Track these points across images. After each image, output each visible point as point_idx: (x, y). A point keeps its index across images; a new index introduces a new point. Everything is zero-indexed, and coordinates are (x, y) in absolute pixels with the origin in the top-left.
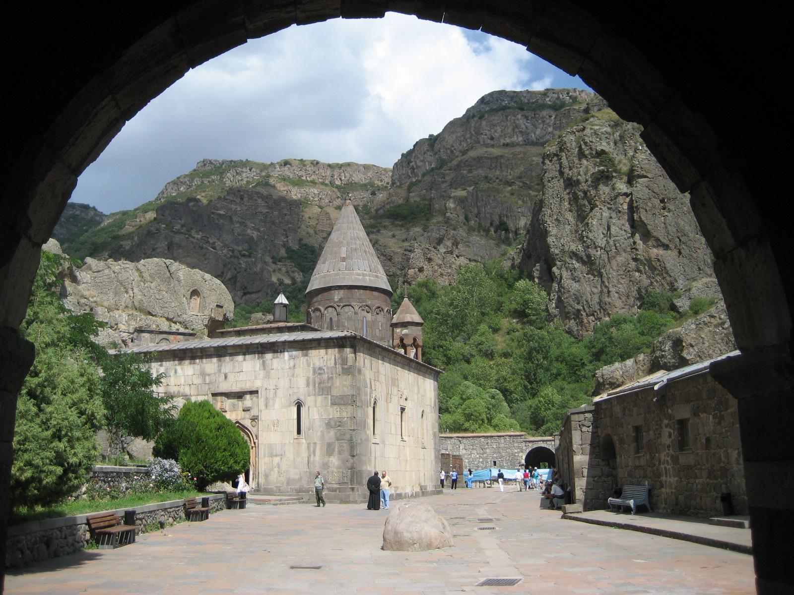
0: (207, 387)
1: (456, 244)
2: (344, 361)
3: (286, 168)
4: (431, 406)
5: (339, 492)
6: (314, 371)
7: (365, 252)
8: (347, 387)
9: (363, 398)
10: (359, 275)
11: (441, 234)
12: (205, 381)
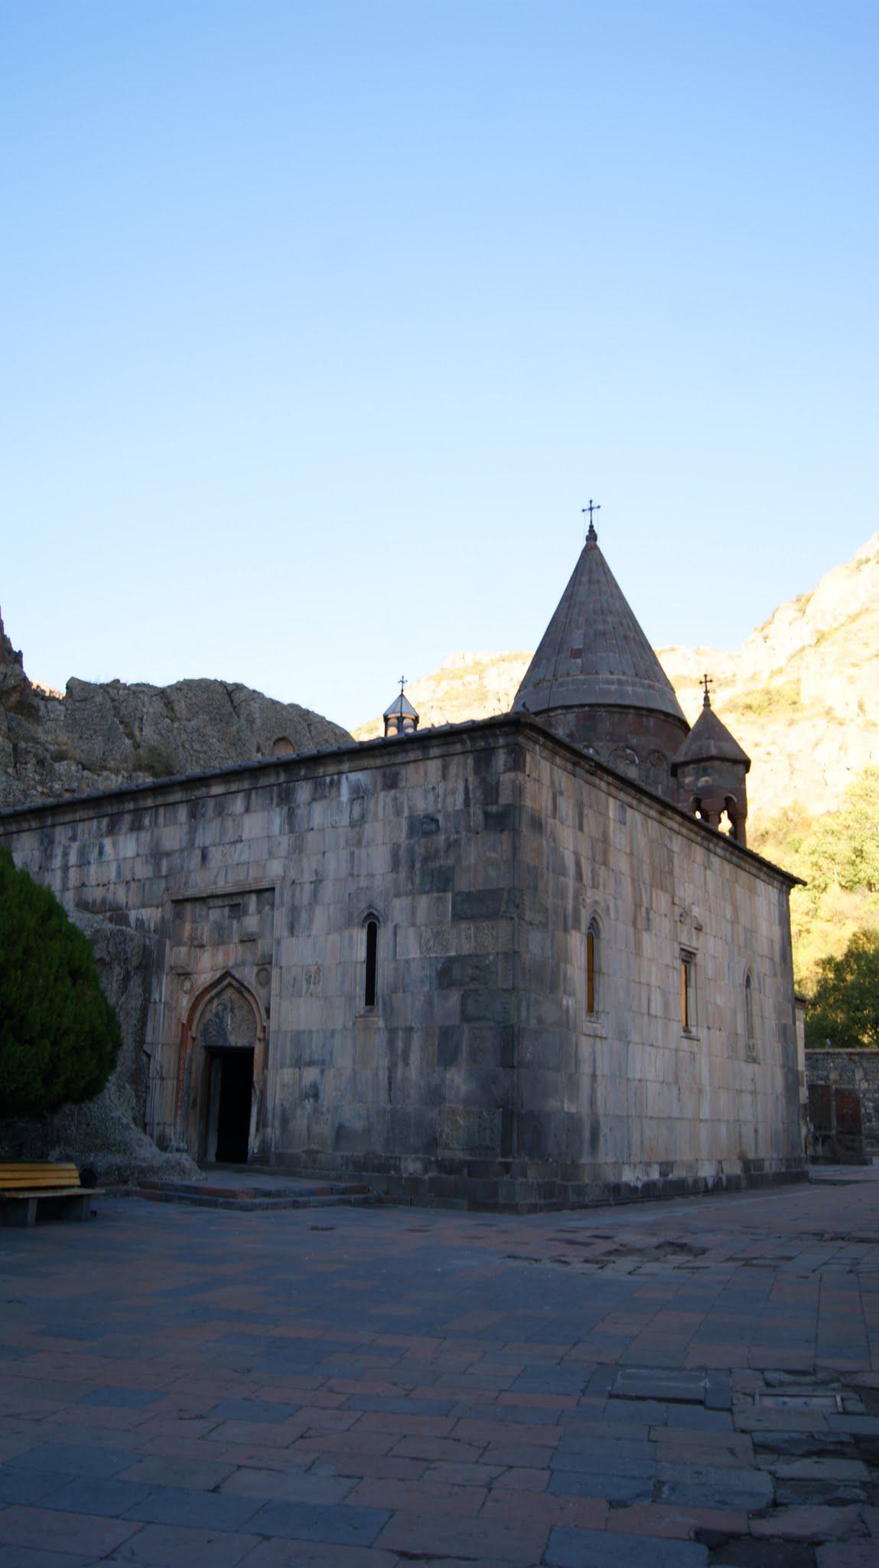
2: (490, 791)
4: (772, 959)
5: (469, 1174)
6: (412, 830)
7: (626, 637)
9: (550, 902)
12: (159, 871)
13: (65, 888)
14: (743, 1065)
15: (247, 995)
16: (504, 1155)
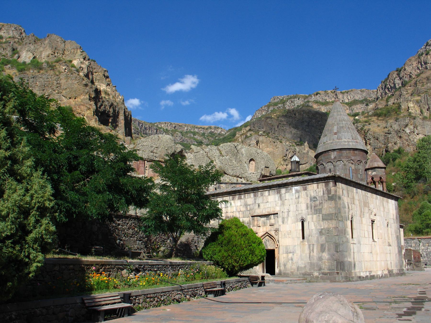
0: (248, 212)
1: (415, 127)
2: (329, 192)
3: (318, 96)
6: (311, 200)
7: (349, 128)
9: (343, 215)
10: (345, 142)
11: (407, 122)
14: (387, 247)
16: (337, 270)
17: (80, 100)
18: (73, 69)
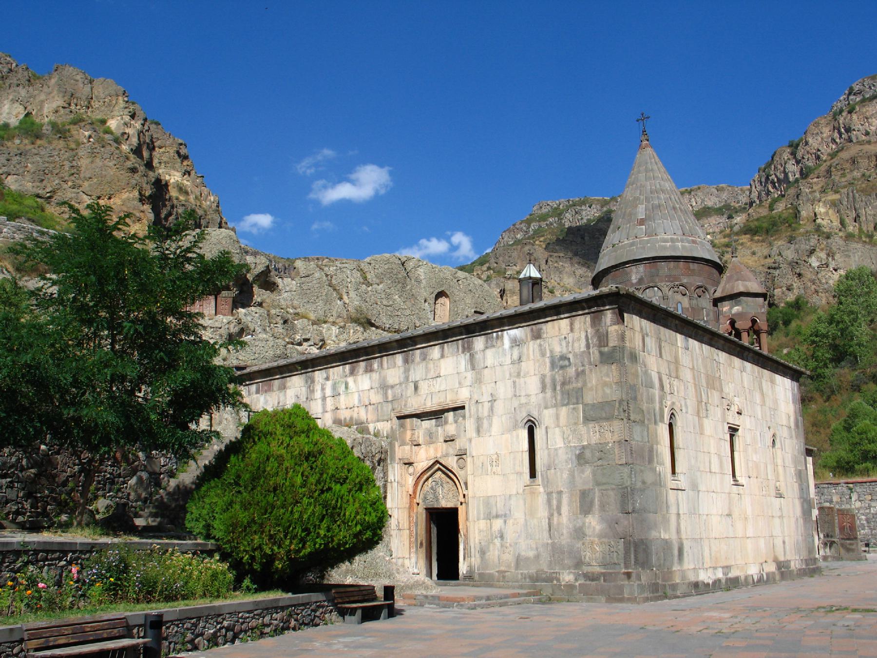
1: (831, 254)
2: (602, 339)
5: (605, 581)
6: (553, 365)
7: (674, 208)
8: (611, 388)
9: (645, 406)
10: (666, 241)
11: (812, 244)
12: (387, 398)
13: (325, 411)
14: (774, 499)
15: (450, 474)
16: (626, 567)
17: (119, 202)
18: (107, 136)
